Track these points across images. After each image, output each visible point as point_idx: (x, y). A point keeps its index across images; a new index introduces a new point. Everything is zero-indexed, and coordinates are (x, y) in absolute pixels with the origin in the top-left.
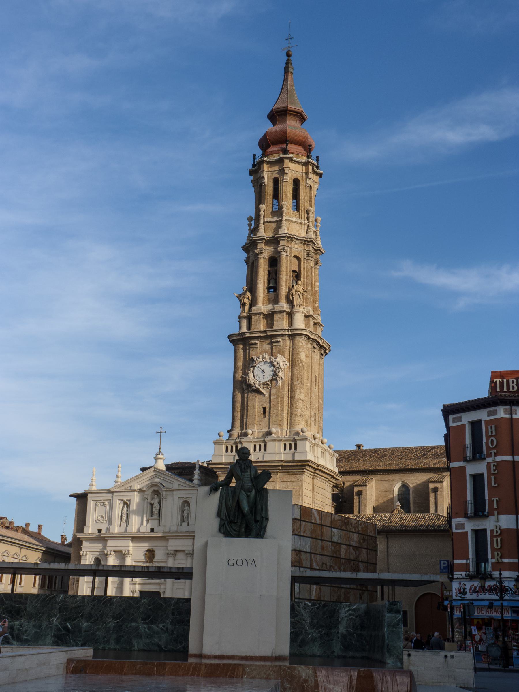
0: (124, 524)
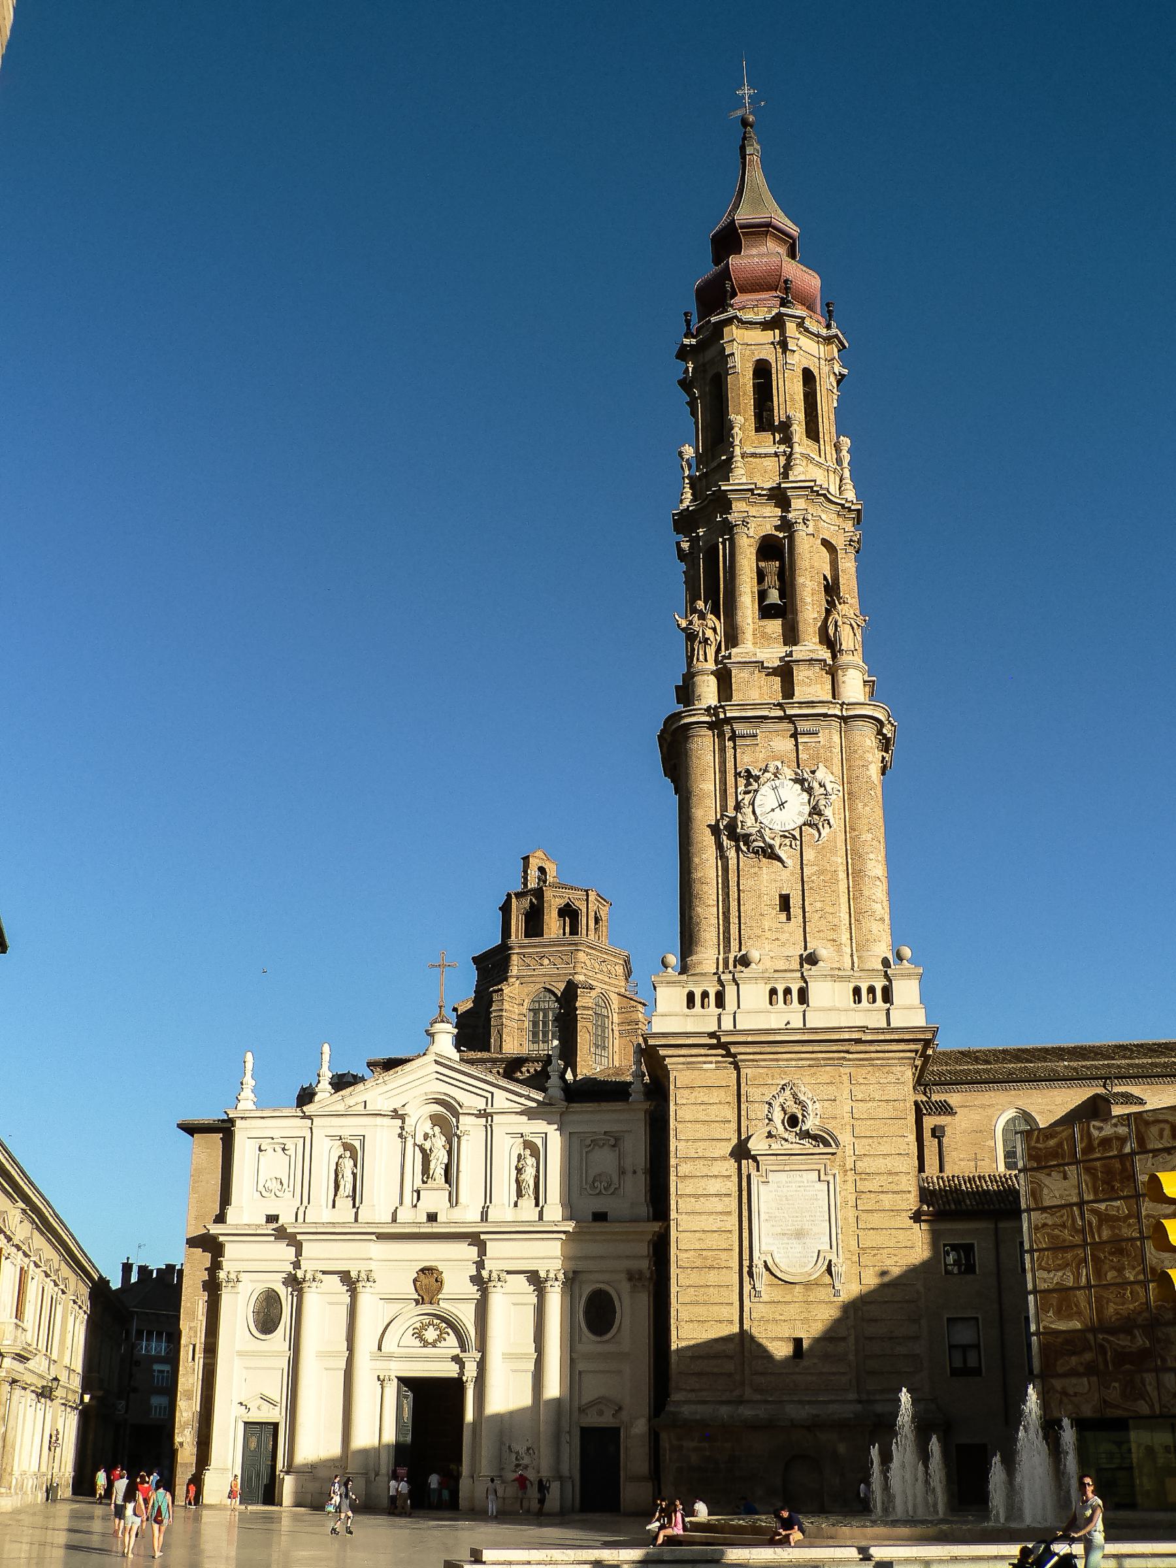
0: (344, 1203)
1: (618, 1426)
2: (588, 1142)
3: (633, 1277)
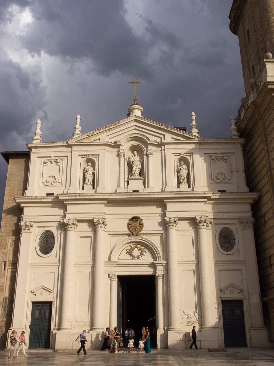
1: (242, 299)
2: (213, 158)
3: (243, 222)
